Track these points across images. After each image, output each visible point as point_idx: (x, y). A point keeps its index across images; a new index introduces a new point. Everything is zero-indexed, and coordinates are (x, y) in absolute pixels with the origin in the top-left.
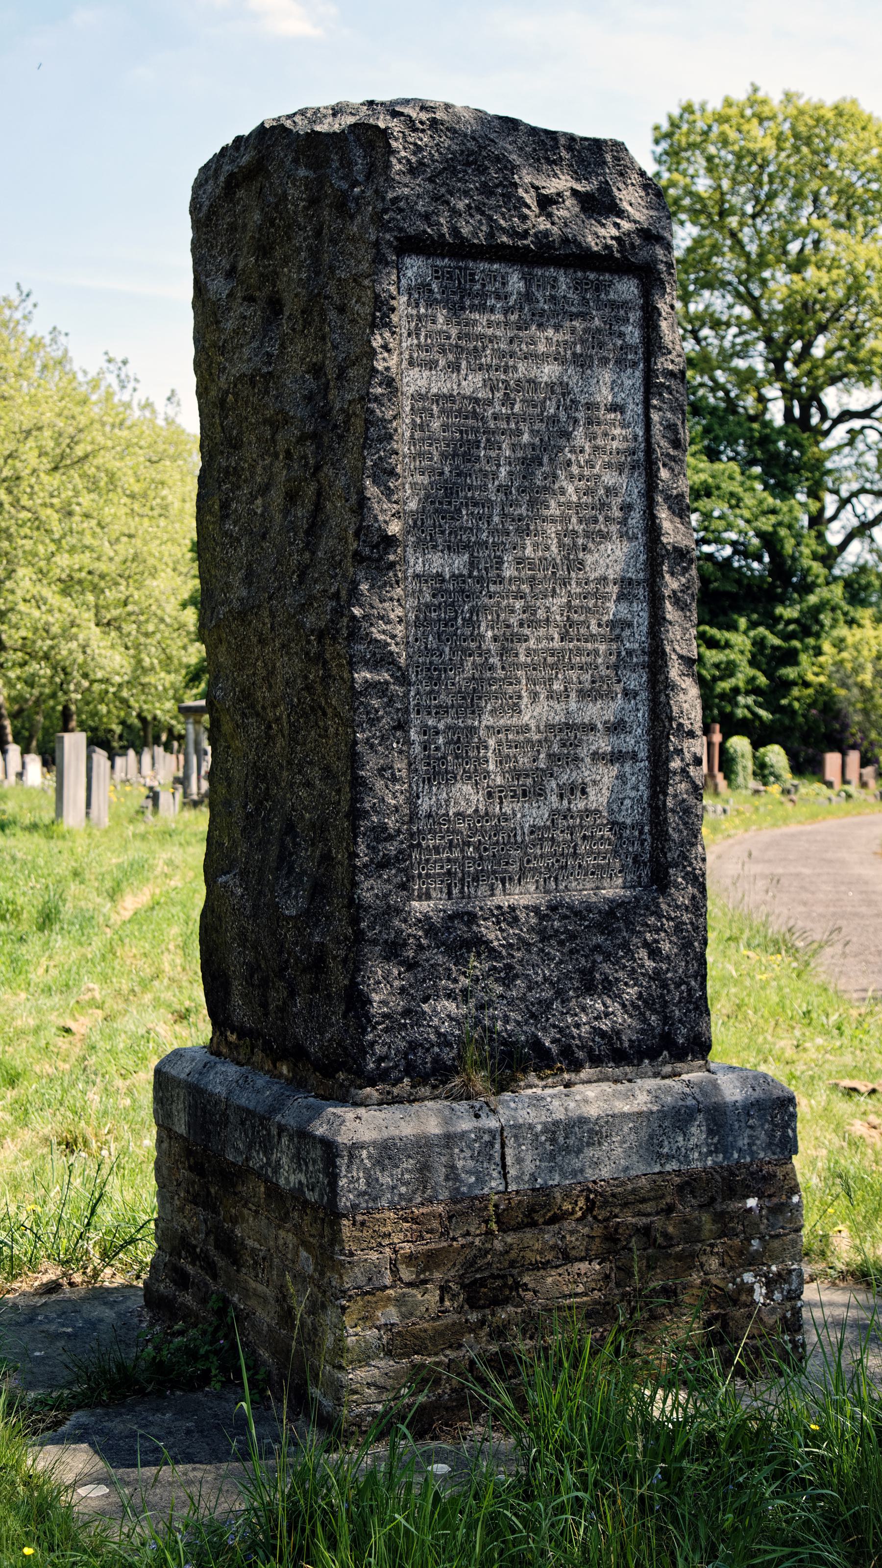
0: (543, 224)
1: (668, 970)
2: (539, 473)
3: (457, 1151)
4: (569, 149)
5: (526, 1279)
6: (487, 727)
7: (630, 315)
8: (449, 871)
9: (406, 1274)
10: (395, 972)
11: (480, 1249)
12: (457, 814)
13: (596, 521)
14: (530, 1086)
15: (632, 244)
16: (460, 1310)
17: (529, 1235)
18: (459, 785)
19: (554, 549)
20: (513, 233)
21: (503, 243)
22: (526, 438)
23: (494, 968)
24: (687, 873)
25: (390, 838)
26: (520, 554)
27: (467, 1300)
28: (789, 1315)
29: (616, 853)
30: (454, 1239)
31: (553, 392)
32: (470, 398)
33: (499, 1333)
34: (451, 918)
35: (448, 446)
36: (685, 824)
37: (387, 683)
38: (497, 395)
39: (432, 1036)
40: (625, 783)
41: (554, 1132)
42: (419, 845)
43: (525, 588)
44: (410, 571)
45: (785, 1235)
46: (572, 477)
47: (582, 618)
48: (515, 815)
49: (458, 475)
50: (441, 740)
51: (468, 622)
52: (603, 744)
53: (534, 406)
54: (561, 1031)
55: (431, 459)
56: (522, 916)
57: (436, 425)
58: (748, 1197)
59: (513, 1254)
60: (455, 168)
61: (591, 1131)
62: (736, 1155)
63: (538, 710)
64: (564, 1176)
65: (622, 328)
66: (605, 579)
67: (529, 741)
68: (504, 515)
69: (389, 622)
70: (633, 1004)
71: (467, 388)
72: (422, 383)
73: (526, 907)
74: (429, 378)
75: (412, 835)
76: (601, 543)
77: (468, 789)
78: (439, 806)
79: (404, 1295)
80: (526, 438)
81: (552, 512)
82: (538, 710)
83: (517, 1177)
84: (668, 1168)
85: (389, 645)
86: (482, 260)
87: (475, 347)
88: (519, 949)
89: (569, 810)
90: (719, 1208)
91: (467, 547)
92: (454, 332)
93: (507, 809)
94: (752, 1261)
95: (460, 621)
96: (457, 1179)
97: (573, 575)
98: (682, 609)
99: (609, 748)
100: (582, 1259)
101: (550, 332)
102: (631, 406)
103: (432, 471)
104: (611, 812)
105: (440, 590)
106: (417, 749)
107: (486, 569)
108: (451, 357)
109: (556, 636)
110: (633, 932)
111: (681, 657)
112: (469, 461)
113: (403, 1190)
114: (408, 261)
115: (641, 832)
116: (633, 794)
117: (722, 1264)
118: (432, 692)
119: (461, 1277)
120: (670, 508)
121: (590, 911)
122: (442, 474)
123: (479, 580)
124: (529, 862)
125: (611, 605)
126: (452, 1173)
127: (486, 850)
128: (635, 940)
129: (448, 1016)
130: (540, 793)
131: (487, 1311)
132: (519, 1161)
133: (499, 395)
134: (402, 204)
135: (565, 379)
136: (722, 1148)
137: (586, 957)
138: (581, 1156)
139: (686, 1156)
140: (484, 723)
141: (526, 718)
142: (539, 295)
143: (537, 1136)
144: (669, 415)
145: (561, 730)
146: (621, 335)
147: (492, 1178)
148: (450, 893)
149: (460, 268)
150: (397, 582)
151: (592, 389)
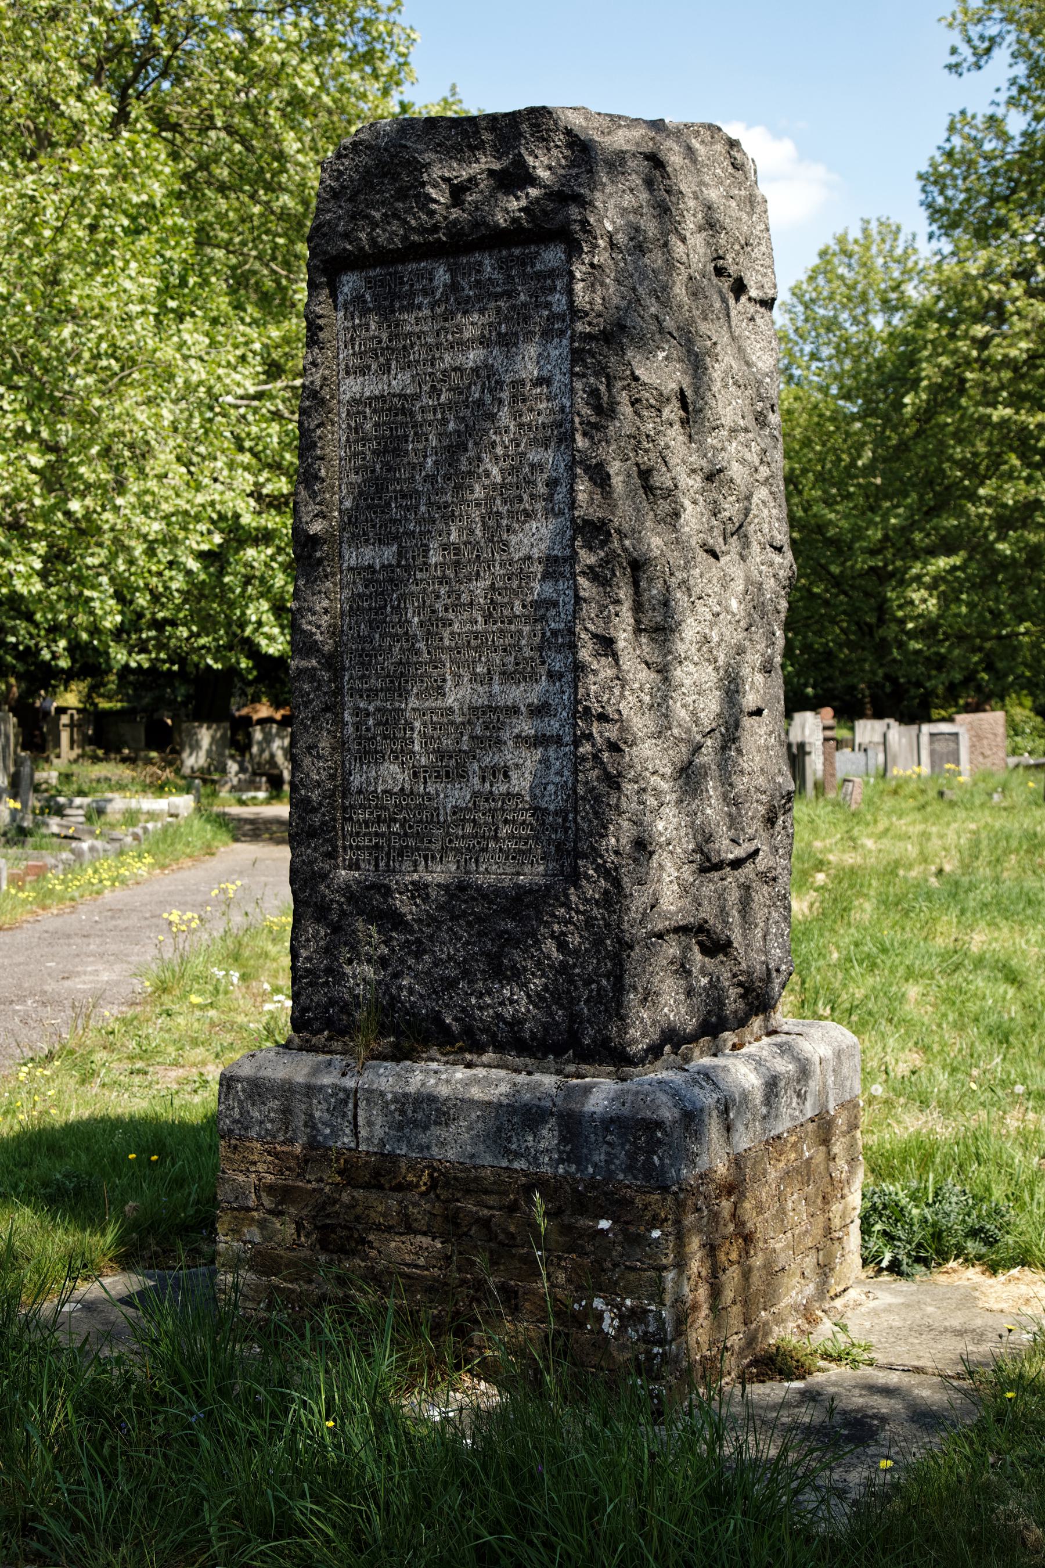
0: (455, 213)
1: (575, 965)
2: (463, 459)
3: (315, 1101)
4: (492, 129)
5: (371, 1237)
6: (413, 709)
7: (558, 283)
8: (377, 844)
9: (267, 1202)
10: (322, 933)
11: (329, 1197)
12: (385, 792)
13: (521, 500)
14: (433, 1060)
15: (545, 213)
16: (312, 1248)
17: (374, 1196)
18: (386, 765)
19: (478, 533)
20: (422, 230)
21: (414, 242)
22: (452, 426)
23: (407, 941)
24: (598, 865)
25: (314, 810)
26: (445, 540)
27: (319, 1241)
28: (642, 1357)
29: (537, 839)
30: (309, 1182)
31: (478, 377)
32: (400, 395)
33: (342, 1281)
34: (368, 888)
35: (379, 444)
36: (596, 813)
37: (314, 669)
38: (425, 388)
39: (346, 996)
40: (548, 768)
41: (403, 1104)
42: (351, 819)
43: (450, 573)
44: (346, 565)
45: (645, 1270)
46: (497, 458)
47: (506, 600)
48: (438, 795)
49: (388, 471)
50: (371, 722)
51: (396, 609)
52: (526, 727)
53: (461, 393)
54: (464, 1010)
55: (364, 459)
56: (433, 895)
57: (368, 426)
58: (602, 1218)
59: (359, 1210)
60: (372, 183)
61: (437, 1110)
62: (591, 1170)
63: (461, 693)
64: (410, 1146)
65: (549, 298)
66: (530, 558)
67: (452, 723)
68: (430, 504)
69: (314, 614)
70: (538, 995)
71: (396, 385)
72: (357, 389)
73: (439, 885)
74: (363, 384)
75: (345, 809)
76: (524, 522)
77: (394, 768)
78: (369, 784)
79: (265, 1220)
80: (452, 426)
81: (476, 495)
82: (461, 693)
83: (367, 1139)
84: (516, 1165)
85: (314, 634)
86: (410, 261)
87: (404, 347)
88: (428, 925)
89: (491, 792)
90: (566, 1220)
91: (396, 538)
92: (384, 336)
93: (431, 789)
94: (608, 1290)
95: (389, 609)
96: (314, 1127)
97: (497, 557)
98: (603, 585)
99: (533, 732)
100: (425, 1234)
101: (475, 317)
103: (365, 468)
104: (534, 796)
105: (371, 581)
106: (350, 730)
107: (413, 557)
108: (382, 360)
109: (480, 619)
110: (541, 921)
111: (595, 636)
112: (398, 456)
113: (269, 1126)
114: (344, 278)
115: (565, 820)
116: (557, 779)
117: (569, 1281)
118: (363, 676)
119: (314, 1217)
120: (591, 479)
121: (497, 896)
122: (373, 471)
123: (407, 568)
124: (451, 841)
125: (536, 586)
126: (310, 1122)
127: (411, 827)
128: (543, 930)
129: (364, 980)
130: (463, 775)
131: (335, 1257)
132: (370, 1124)
133: (425, 388)
134: (325, 229)
135: (490, 361)
136: (574, 1157)
137: (493, 940)
138: (428, 1133)
139: (536, 1159)
140: (410, 705)
141: (450, 701)
142: (464, 283)
143: (387, 1104)
144: (592, 380)
145: (484, 713)
146: (548, 305)
147: (345, 1134)
148: (377, 866)
149: (390, 274)
150: (326, 576)
151: (518, 366)
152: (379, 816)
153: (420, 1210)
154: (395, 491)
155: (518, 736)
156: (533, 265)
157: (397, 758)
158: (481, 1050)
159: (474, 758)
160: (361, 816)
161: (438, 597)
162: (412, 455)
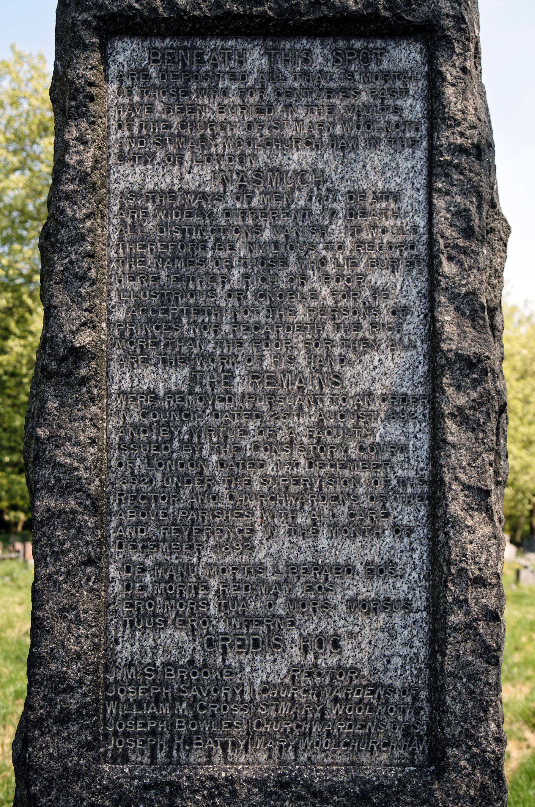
2: (283, 274)
26: (256, 367)
32: (196, 193)
35: (166, 247)
43: (263, 406)
46: (327, 278)
49: (177, 279)
55: (144, 263)
57: (151, 224)
63: (275, 546)
68: (235, 324)
74: (144, 174)
80: (266, 235)
81: (299, 318)
86: (212, 36)
89: (316, 665)
92: (176, 120)
95: (176, 443)
103: (144, 276)
107: (212, 384)
108: (171, 148)
112: (192, 263)
122: (156, 279)
133: (232, 188)
141: (261, 556)
149: (185, 49)
154: (187, 304)
159: (293, 624)
161: (245, 432)
162: (211, 264)
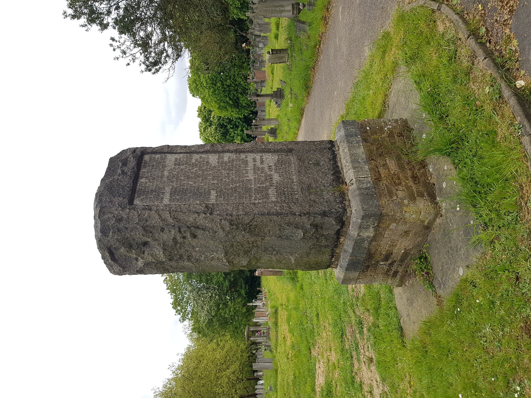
8: (290, 194)
18: (269, 192)
44: (215, 203)
49: (191, 192)
55: (186, 198)
57: (178, 197)
77: (270, 190)
93: (275, 182)
102: (176, 156)
105: (220, 196)
106: (260, 201)
116: (271, 156)
148: (296, 194)
149: (138, 192)
152: (283, 194)
153: (380, 161)
154: (197, 191)
155: (261, 164)
156: (148, 161)
157: (267, 190)
158: (338, 167)
160: (283, 198)
161: (226, 181)
